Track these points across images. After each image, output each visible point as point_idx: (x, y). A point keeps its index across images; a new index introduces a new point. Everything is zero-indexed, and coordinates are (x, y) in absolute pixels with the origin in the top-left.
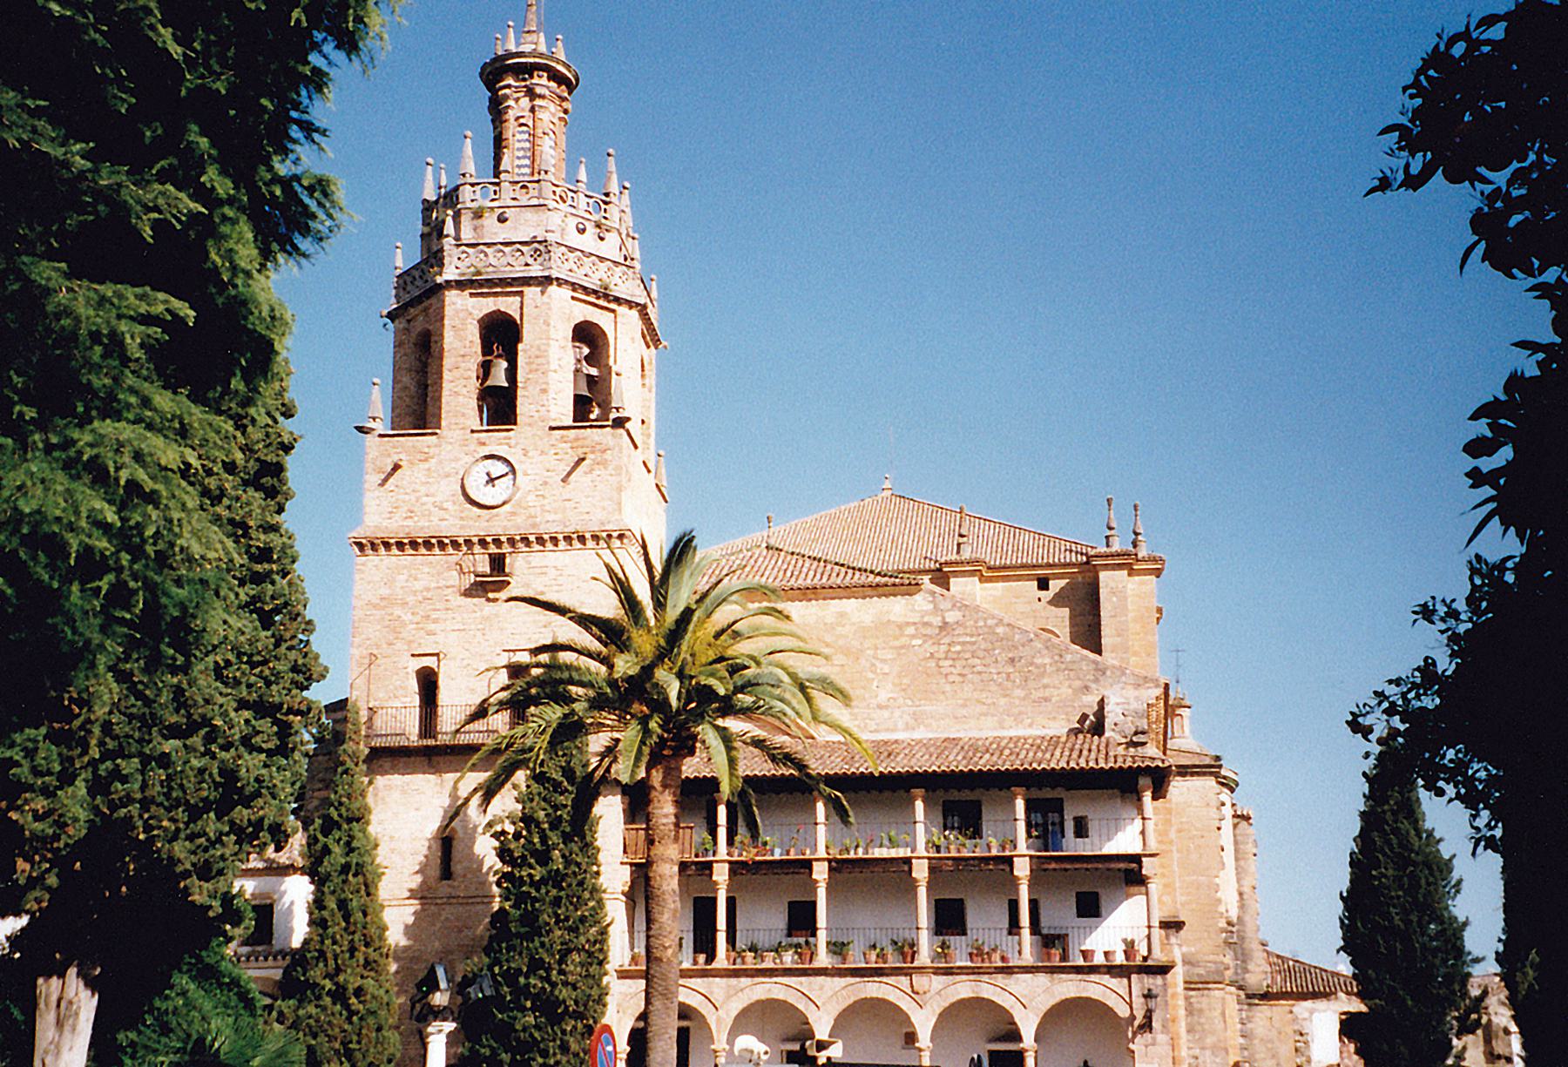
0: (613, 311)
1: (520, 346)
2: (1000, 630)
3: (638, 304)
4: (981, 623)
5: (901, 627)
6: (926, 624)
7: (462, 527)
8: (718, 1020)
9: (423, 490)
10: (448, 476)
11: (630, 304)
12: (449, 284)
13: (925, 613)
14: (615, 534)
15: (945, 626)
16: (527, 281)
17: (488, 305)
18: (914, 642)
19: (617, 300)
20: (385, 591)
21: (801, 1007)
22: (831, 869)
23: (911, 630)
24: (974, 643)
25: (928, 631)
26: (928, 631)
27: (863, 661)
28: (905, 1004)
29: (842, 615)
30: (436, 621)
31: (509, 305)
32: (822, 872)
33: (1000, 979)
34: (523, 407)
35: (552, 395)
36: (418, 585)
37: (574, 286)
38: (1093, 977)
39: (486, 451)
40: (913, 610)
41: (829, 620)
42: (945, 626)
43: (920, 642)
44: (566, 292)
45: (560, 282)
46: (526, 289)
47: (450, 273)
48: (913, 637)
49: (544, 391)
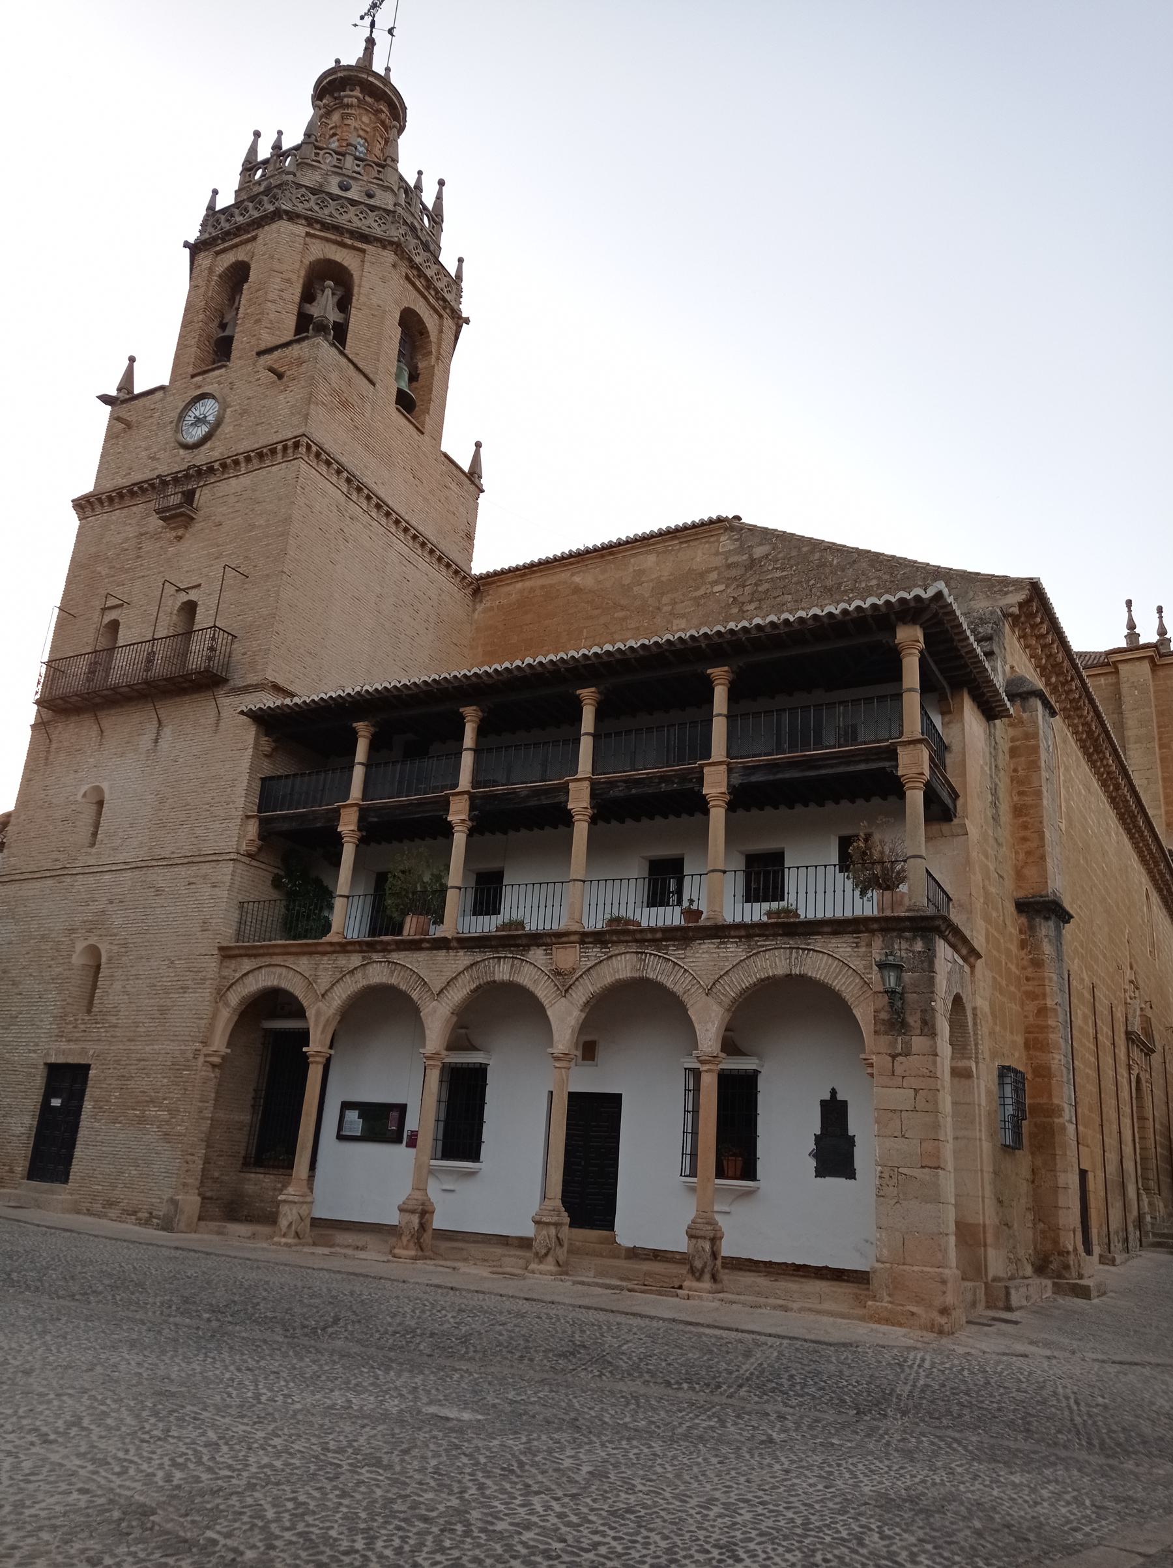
0: (363, 251)
1: (245, 286)
2: (817, 556)
3: (391, 243)
4: (794, 553)
5: (702, 575)
6: (729, 566)
8: (318, 1014)
11: (384, 243)
13: (727, 554)
14: (290, 443)
15: (752, 563)
18: (716, 589)
19: (365, 238)
20: (93, 550)
21: (415, 995)
22: (472, 808)
23: (714, 576)
24: (785, 577)
25: (734, 573)
26: (734, 573)
27: (658, 620)
28: (543, 991)
29: (641, 572)
32: (458, 812)
33: (674, 954)
35: (265, 323)
37: (310, 221)
38: (818, 943)
39: (198, 392)
40: (717, 553)
41: (626, 582)
42: (752, 563)
43: (721, 587)
44: (300, 229)
45: (292, 217)
48: (716, 582)
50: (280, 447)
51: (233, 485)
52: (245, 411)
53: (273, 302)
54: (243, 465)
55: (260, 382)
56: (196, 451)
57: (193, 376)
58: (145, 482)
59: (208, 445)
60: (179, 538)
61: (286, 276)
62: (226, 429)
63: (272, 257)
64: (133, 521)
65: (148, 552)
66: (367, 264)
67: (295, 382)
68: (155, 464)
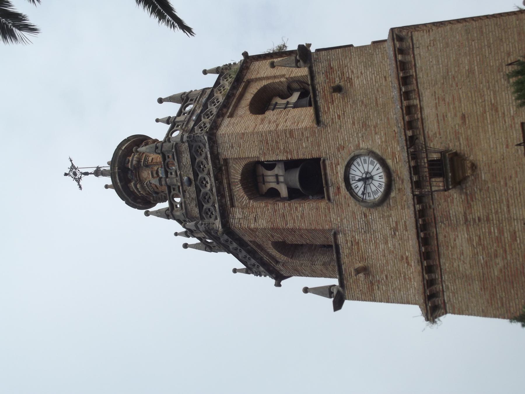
7: (409, 207)
9: (382, 246)
10: (368, 223)
12: (225, 224)
14: (398, 45)
16: (215, 157)
17: (238, 190)
20: (477, 285)
30: (501, 232)
31: (236, 172)
34: (304, 151)
35: (294, 127)
36: (468, 251)
45: (215, 126)
46: (222, 157)
47: (218, 224)
49: (291, 132)
50: (400, 57)
51: (429, 111)
52: (365, 125)
53: (277, 125)
54: (411, 102)
55: (340, 113)
56: (394, 175)
57: (329, 199)
58: (417, 222)
59: (389, 162)
60: (474, 167)
61: (259, 121)
62: (376, 143)
63: (243, 134)
64: (452, 237)
65: (484, 206)
66: (259, 76)
67: (345, 70)
68: (401, 227)
